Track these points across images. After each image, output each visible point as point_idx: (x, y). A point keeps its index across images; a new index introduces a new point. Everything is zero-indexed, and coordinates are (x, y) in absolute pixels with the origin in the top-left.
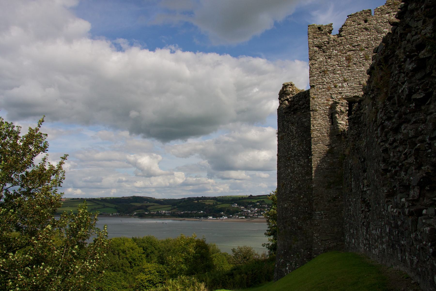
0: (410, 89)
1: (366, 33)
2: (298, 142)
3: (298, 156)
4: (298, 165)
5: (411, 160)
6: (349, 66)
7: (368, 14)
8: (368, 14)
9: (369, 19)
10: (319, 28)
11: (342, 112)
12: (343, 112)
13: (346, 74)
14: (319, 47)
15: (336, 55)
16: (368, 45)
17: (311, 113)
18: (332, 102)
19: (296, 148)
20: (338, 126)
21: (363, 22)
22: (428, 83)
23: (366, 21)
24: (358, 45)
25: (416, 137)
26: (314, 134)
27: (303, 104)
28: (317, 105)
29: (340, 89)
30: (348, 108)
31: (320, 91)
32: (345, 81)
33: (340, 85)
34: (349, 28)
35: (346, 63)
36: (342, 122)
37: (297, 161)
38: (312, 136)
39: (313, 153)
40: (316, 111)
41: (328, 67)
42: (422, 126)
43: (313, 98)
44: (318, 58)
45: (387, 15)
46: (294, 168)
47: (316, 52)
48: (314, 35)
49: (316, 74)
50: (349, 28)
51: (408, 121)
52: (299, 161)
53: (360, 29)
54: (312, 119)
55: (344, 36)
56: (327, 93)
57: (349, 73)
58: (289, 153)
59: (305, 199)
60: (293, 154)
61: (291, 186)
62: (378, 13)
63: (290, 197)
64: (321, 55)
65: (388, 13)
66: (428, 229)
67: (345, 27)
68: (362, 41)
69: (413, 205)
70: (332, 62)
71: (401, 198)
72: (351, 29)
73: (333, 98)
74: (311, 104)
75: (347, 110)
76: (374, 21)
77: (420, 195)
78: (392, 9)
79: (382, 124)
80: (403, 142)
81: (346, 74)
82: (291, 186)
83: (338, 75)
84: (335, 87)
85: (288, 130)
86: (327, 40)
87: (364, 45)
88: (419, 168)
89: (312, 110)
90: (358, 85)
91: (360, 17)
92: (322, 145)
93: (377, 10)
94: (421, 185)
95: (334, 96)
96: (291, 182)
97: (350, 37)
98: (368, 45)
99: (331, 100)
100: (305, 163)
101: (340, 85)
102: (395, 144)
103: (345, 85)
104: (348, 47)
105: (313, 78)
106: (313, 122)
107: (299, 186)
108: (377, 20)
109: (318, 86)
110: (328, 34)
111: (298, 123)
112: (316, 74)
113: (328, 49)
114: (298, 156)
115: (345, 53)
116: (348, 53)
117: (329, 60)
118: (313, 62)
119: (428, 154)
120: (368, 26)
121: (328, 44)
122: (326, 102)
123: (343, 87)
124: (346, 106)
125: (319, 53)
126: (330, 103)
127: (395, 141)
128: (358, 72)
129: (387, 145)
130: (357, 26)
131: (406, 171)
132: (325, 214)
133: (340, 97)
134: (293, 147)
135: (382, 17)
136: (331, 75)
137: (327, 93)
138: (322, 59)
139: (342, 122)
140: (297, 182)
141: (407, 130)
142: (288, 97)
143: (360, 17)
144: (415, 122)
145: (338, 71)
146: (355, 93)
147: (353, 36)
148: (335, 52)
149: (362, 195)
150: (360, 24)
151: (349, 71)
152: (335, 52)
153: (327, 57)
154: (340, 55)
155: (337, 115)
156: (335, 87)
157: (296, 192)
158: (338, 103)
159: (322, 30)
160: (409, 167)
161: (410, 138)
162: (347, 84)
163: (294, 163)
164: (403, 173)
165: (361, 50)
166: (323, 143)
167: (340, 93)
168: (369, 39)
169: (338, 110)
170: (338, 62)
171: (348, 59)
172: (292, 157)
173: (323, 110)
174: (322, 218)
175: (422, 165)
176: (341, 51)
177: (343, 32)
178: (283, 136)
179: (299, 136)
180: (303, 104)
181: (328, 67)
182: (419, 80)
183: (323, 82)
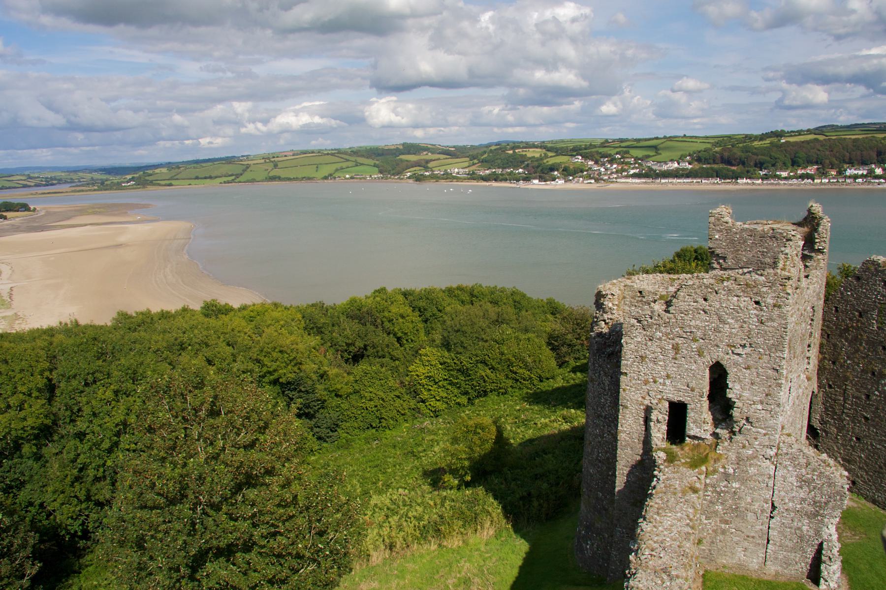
6: (676, 359)
9: (711, 297)
10: (640, 292)
13: (672, 369)
14: (639, 322)
15: (660, 339)
17: (621, 407)
21: (701, 301)
23: (705, 300)
26: (622, 436)
30: (667, 418)
32: (668, 376)
33: (661, 381)
34: (681, 303)
35: (671, 353)
36: (658, 435)
40: (626, 407)
43: (624, 390)
45: (735, 299)
47: (633, 326)
50: (681, 303)
60: (603, 414)
62: (723, 292)
70: (654, 346)
81: (672, 369)
84: (655, 382)
90: (685, 387)
91: (698, 291)
95: (652, 394)
99: (648, 398)
101: (661, 381)
103: (668, 382)
107: (608, 458)
113: (650, 326)
116: (677, 340)
117: (649, 343)
120: (708, 307)
122: (640, 399)
123: (664, 384)
128: (687, 369)
130: (692, 303)
133: (659, 397)
136: (651, 365)
139: (658, 435)
140: (606, 452)
143: (698, 291)
148: (659, 334)
150: (697, 302)
152: (659, 334)
165: (694, 340)
171: (676, 348)
176: (667, 334)
177: (673, 308)
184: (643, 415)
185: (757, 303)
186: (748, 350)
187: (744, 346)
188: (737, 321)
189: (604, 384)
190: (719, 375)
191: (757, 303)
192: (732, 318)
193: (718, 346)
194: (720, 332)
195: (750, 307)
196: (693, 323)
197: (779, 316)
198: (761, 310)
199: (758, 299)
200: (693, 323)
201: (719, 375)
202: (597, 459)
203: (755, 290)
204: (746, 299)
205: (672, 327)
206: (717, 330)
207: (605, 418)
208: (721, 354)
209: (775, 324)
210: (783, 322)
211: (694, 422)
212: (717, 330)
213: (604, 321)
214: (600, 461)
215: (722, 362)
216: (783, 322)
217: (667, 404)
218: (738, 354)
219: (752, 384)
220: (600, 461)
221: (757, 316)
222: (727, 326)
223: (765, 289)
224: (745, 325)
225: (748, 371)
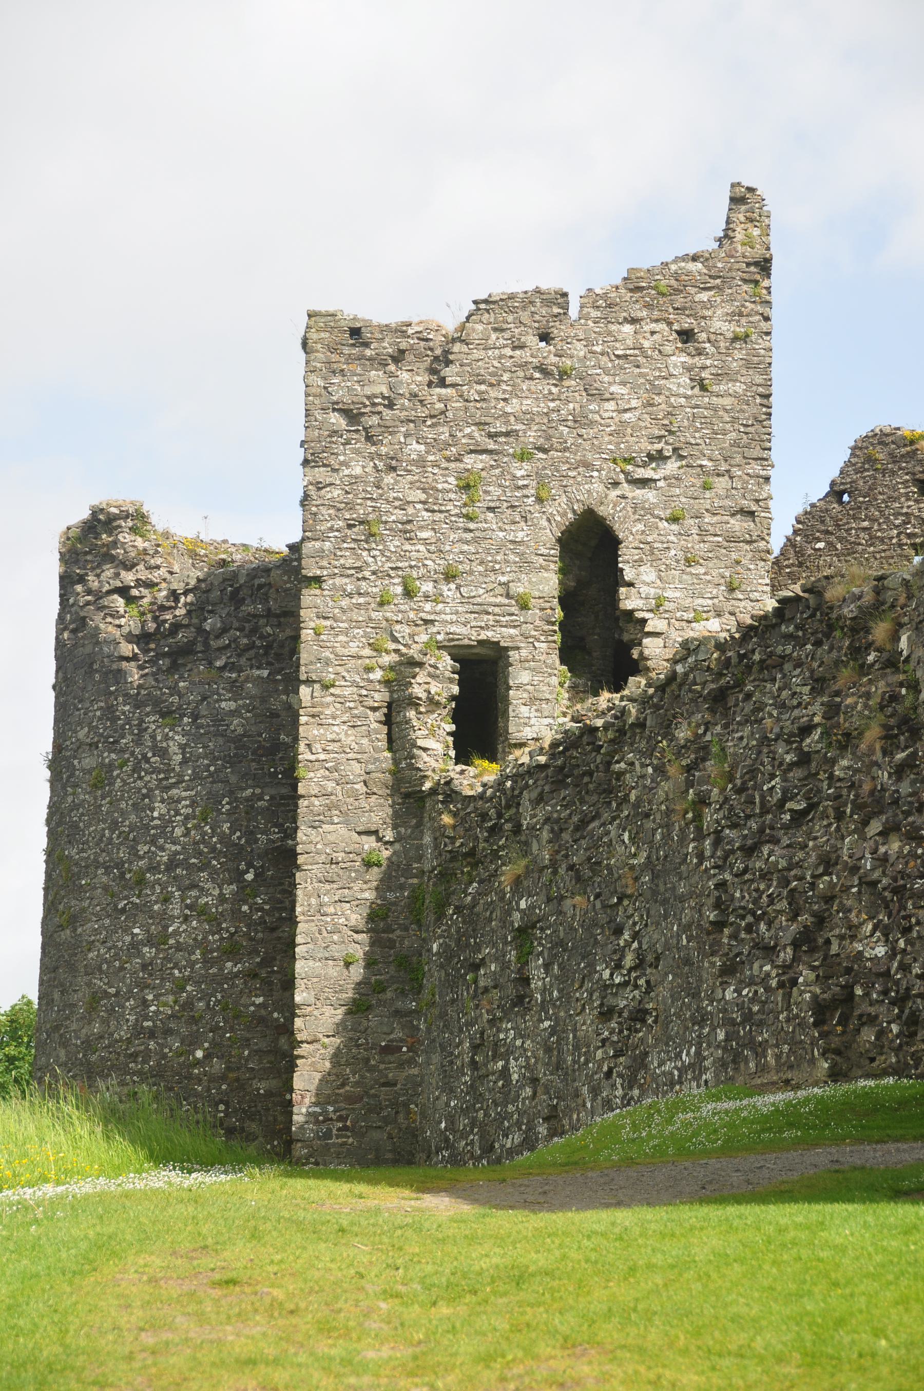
0: (785, 791)
1: (546, 386)
2: (193, 804)
3: (189, 867)
4: (187, 907)
5: (783, 905)
6: (469, 518)
7: (556, 310)
8: (556, 310)
10: (355, 332)
11: (433, 703)
12: (438, 704)
14: (352, 416)
15: (421, 462)
16: (549, 438)
18: (395, 658)
19: (178, 832)
20: (413, 757)
21: (532, 340)
22: (812, 789)
23: (545, 337)
24: (507, 434)
25: (789, 869)
26: (312, 783)
27: (224, 630)
28: (328, 663)
29: (428, 607)
30: (456, 690)
31: (345, 603)
32: (449, 577)
33: (427, 587)
34: (477, 354)
35: (455, 503)
37: (183, 890)
38: (301, 790)
39: (301, 860)
41: (385, 507)
42: (801, 855)
44: (346, 464)
45: (628, 328)
46: (164, 919)
48: (334, 357)
49: (331, 529)
50: (477, 354)
51: (776, 841)
52: (194, 893)
53: (524, 365)
54: (303, 719)
55: (453, 385)
56: (374, 615)
57: (467, 542)
58: (143, 849)
59: (217, 1066)
61: (145, 1003)
62: (595, 314)
63: (134, 1056)
64: (357, 452)
65: (633, 321)
66: (808, 995)
67: (465, 348)
68: (528, 418)
69: (784, 973)
70: (401, 486)
71: (761, 967)
72: (486, 360)
73: (395, 640)
74: (304, 657)
75: (453, 698)
76: (579, 345)
77: (793, 960)
78: (648, 306)
79: (717, 832)
80: (765, 876)
81: (456, 550)
82: (145, 1003)
83: (422, 548)
85: (138, 742)
86: (385, 391)
87: (532, 436)
88: (793, 918)
89: (309, 682)
91: (525, 316)
92: (342, 830)
93: (591, 298)
94: (796, 944)
95: (401, 631)
96: (144, 986)
97: (480, 393)
98: (549, 438)
100: (222, 899)
102: (747, 877)
103: (449, 590)
104: (470, 436)
105: (317, 544)
106: (308, 730)
107: (188, 1005)
108: (589, 343)
109: (338, 581)
110: (392, 367)
111: (195, 717)
112: (331, 529)
113: (388, 429)
114: (189, 867)
115: (457, 460)
117: (389, 479)
118: (320, 474)
119: (808, 898)
121: (391, 406)
122: (367, 652)
123: (438, 598)
124: (451, 680)
125: (347, 443)
126: (386, 659)
127: (745, 871)
129: (727, 876)
130: (508, 352)
131: (769, 924)
132: (341, 1119)
134: (167, 822)
135: (610, 333)
136: (393, 544)
137: (374, 615)
138: (358, 471)
141: (773, 855)
142: (129, 578)
143: (525, 316)
144: (788, 846)
145: (421, 528)
146: (487, 627)
147: (493, 393)
148: (415, 448)
149: (603, 998)
150: (522, 347)
151: (469, 536)
152: (415, 448)
153: (381, 465)
154: (436, 465)
155: (411, 714)
156: (409, 593)
157: (168, 1032)
158: (420, 665)
159: (366, 345)
160: (776, 917)
161: (780, 871)
162: (458, 588)
163: (166, 900)
164: (763, 927)
165: (523, 457)
166: (346, 823)
167: (426, 622)
168: (554, 416)
169: (418, 691)
170: (424, 490)
172: (153, 869)
173: (355, 684)
174: (328, 1135)
175: (797, 915)
178: (111, 767)
179: (196, 777)
180: (224, 630)
181: (385, 507)
182: (799, 780)
183: (359, 569)
184: (380, 697)
185: (686, 336)
186: (672, 466)
187: (658, 458)
188: (634, 388)
189: (163, 753)
190: (591, 551)
191: (686, 336)
192: (623, 383)
193: (588, 465)
194: (592, 423)
195: (668, 349)
196: (513, 407)
197: (749, 365)
198: (700, 352)
199: (687, 323)
200: (513, 407)
201: (591, 551)
202: (138, 1031)
203: (679, 301)
204: (653, 326)
205: (456, 424)
206: (580, 421)
207: (171, 865)
208: (598, 487)
209: (739, 388)
210: (759, 379)
211: (532, 701)
212: (580, 421)
213: (123, 591)
214: (152, 1034)
215: (602, 511)
216: (759, 379)
217: (446, 662)
218: (644, 483)
219: (689, 562)
220: (152, 1034)
221: (689, 370)
222: (611, 405)
223: (704, 296)
224: (658, 399)
225: (675, 527)
